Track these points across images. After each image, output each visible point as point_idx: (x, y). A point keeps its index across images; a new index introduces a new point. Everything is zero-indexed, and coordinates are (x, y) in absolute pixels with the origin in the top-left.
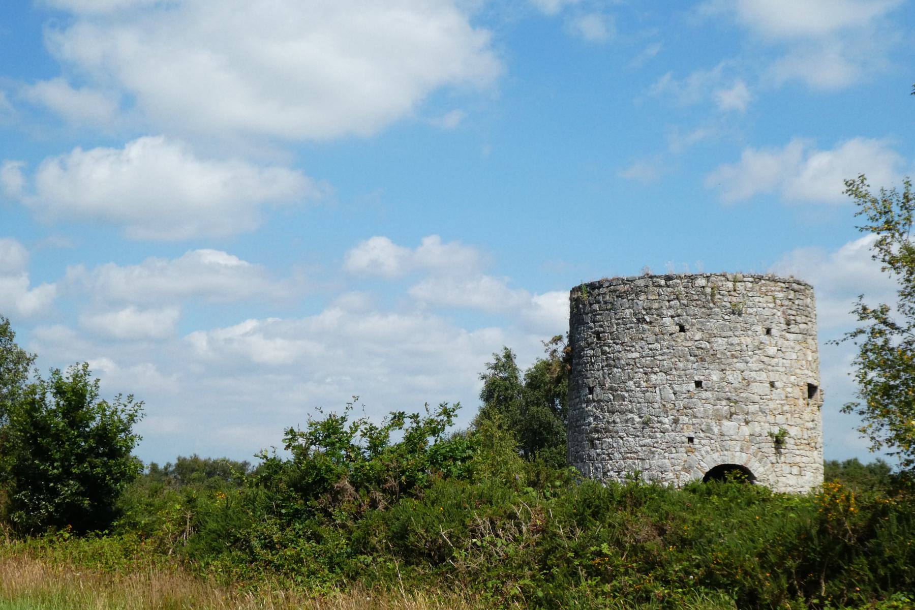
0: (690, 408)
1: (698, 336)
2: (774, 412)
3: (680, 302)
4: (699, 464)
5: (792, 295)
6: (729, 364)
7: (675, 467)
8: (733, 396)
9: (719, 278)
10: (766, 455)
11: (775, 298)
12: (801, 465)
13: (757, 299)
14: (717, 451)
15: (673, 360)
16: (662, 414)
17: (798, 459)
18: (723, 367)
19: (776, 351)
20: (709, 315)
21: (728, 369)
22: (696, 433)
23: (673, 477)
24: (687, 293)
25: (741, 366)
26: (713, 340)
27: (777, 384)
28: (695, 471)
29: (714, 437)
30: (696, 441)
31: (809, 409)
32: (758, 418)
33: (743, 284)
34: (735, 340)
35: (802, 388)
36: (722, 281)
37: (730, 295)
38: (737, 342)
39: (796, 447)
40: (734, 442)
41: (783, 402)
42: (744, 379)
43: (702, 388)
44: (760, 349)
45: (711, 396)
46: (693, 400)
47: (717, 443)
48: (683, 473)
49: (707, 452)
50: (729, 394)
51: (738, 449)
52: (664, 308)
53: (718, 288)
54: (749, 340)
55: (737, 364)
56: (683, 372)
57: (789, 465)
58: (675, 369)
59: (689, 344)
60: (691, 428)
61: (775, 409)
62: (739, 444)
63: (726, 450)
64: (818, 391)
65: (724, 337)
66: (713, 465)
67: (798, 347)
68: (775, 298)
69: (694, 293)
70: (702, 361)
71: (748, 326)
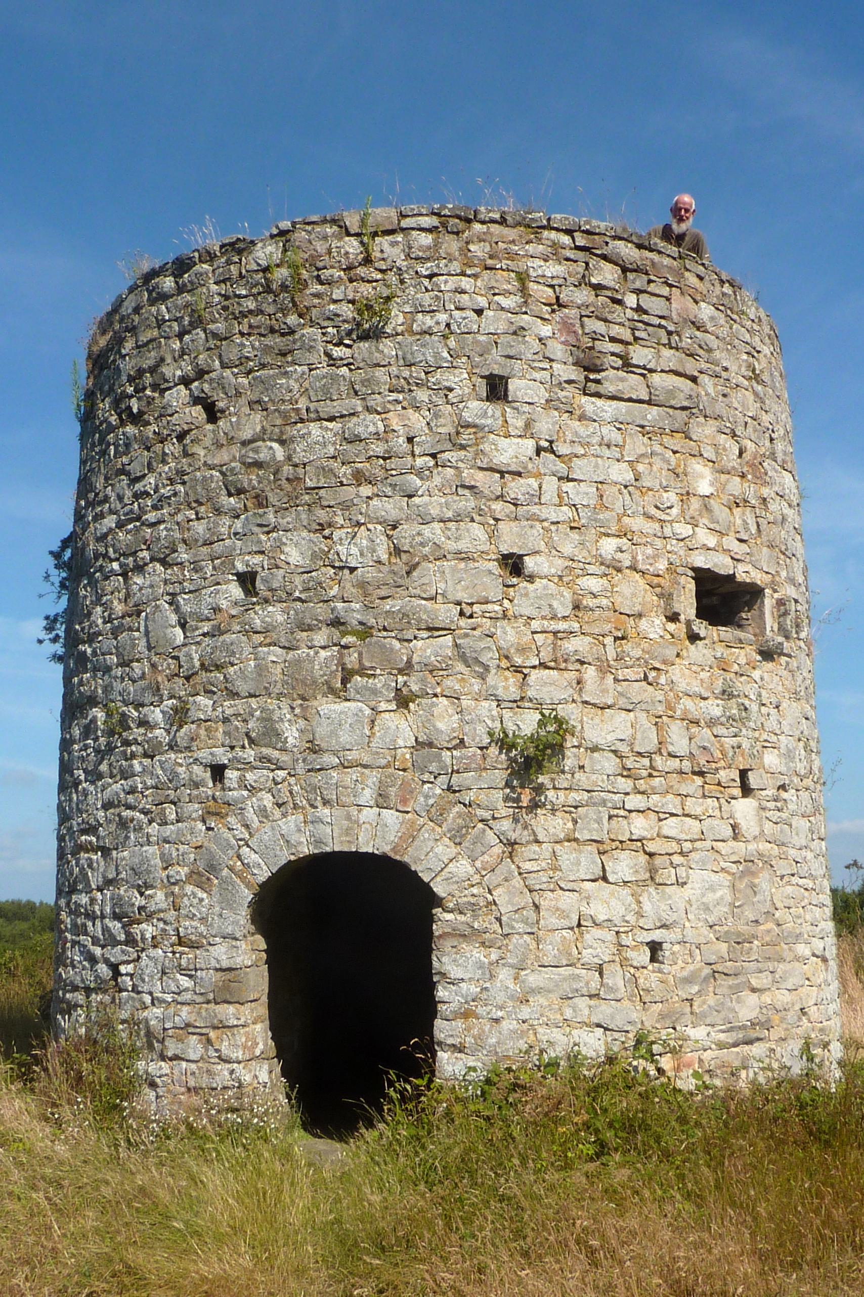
0: (218, 667)
1: (253, 424)
2: (518, 660)
3: (205, 330)
4: (239, 857)
5: (607, 274)
6: (346, 506)
7: (171, 871)
8: (355, 612)
9: (318, 229)
10: (481, 813)
11: (523, 278)
12: (651, 847)
13: (451, 283)
14: (296, 807)
15: (179, 517)
16: (148, 698)
17: (640, 826)
18: (322, 515)
19: (531, 452)
20: (284, 355)
21: (340, 520)
22: (232, 748)
23: (164, 906)
24: (226, 297)
25: (389, 507)
26: (292, 431)
27: (530, 563)
28: (223, 881)
29: (285, 758)
30: (231, 775)
31: (697, 652)
32: (448, 682)
33: (399, 238)
34: (368, 424)
35: (656, 580)
36: (325, 238)
37: (351, 281)
38: (372, 429)
39: (624, 784)
40: (354, 774)
41: (562, 626)
42: (397, 551)
43: (256, 594)
44: (463, 447)
45: (280, 618)
46: (228, 638)
47: (292, 780)
48: (189, 889)
49: (263, 813)
50: (340, 605)
51: (367, 795)
52: (169, 360)
53: (313, 262)
54: (417, 421)
55: (375, 502)
56: (205, 550)
57: (593, 848)
58: (184, 541)
59: (223, 456)
60: (220, 735)
61: (522, 650)
62: (373, 777)
63: (326, 803)
64: (769, 603)
65: (331, 419)
66: (285, 857)
67: (637, 445)
68: (523, 278)
69: (244, 292)
70: (260, 505)
71: (417, 373)
